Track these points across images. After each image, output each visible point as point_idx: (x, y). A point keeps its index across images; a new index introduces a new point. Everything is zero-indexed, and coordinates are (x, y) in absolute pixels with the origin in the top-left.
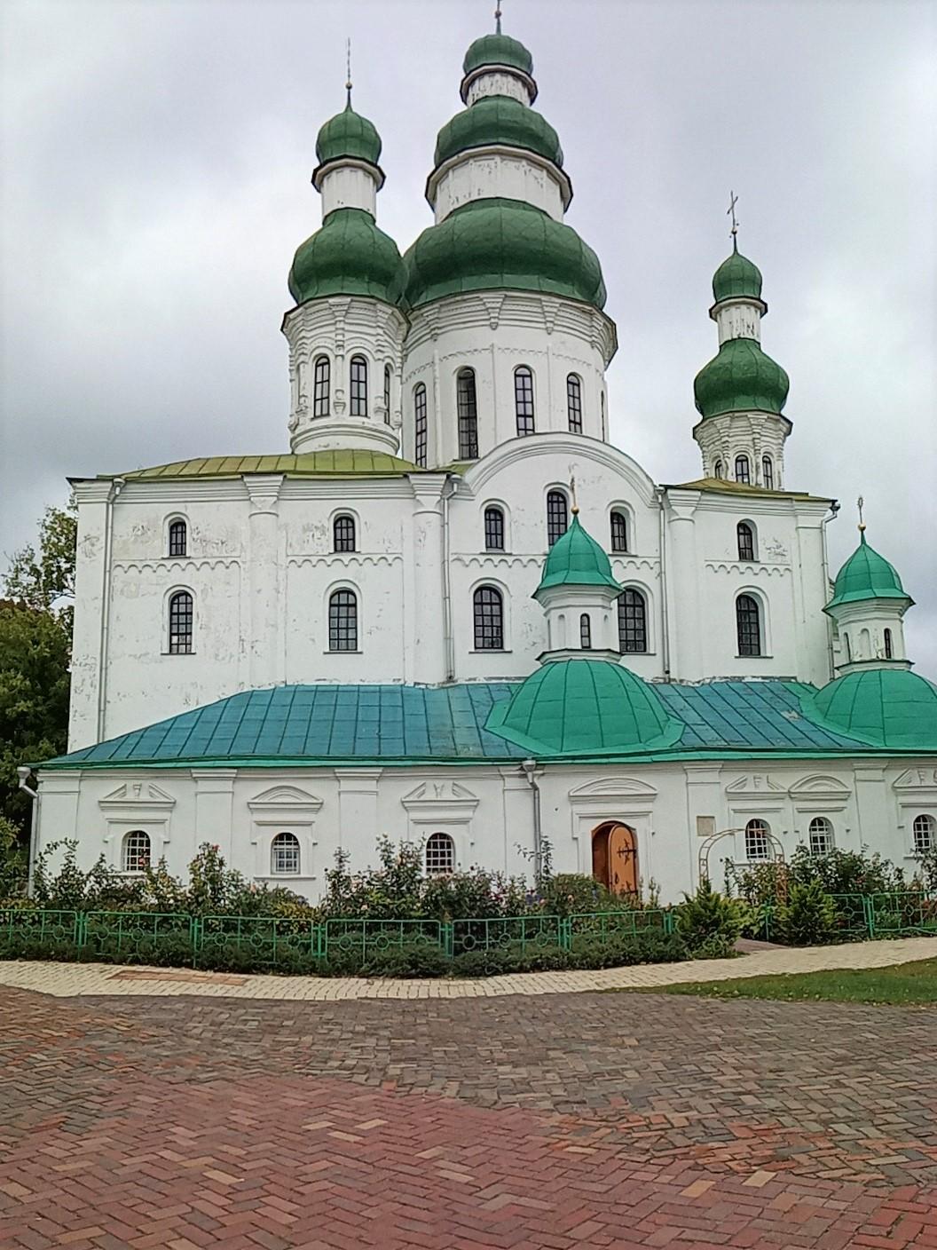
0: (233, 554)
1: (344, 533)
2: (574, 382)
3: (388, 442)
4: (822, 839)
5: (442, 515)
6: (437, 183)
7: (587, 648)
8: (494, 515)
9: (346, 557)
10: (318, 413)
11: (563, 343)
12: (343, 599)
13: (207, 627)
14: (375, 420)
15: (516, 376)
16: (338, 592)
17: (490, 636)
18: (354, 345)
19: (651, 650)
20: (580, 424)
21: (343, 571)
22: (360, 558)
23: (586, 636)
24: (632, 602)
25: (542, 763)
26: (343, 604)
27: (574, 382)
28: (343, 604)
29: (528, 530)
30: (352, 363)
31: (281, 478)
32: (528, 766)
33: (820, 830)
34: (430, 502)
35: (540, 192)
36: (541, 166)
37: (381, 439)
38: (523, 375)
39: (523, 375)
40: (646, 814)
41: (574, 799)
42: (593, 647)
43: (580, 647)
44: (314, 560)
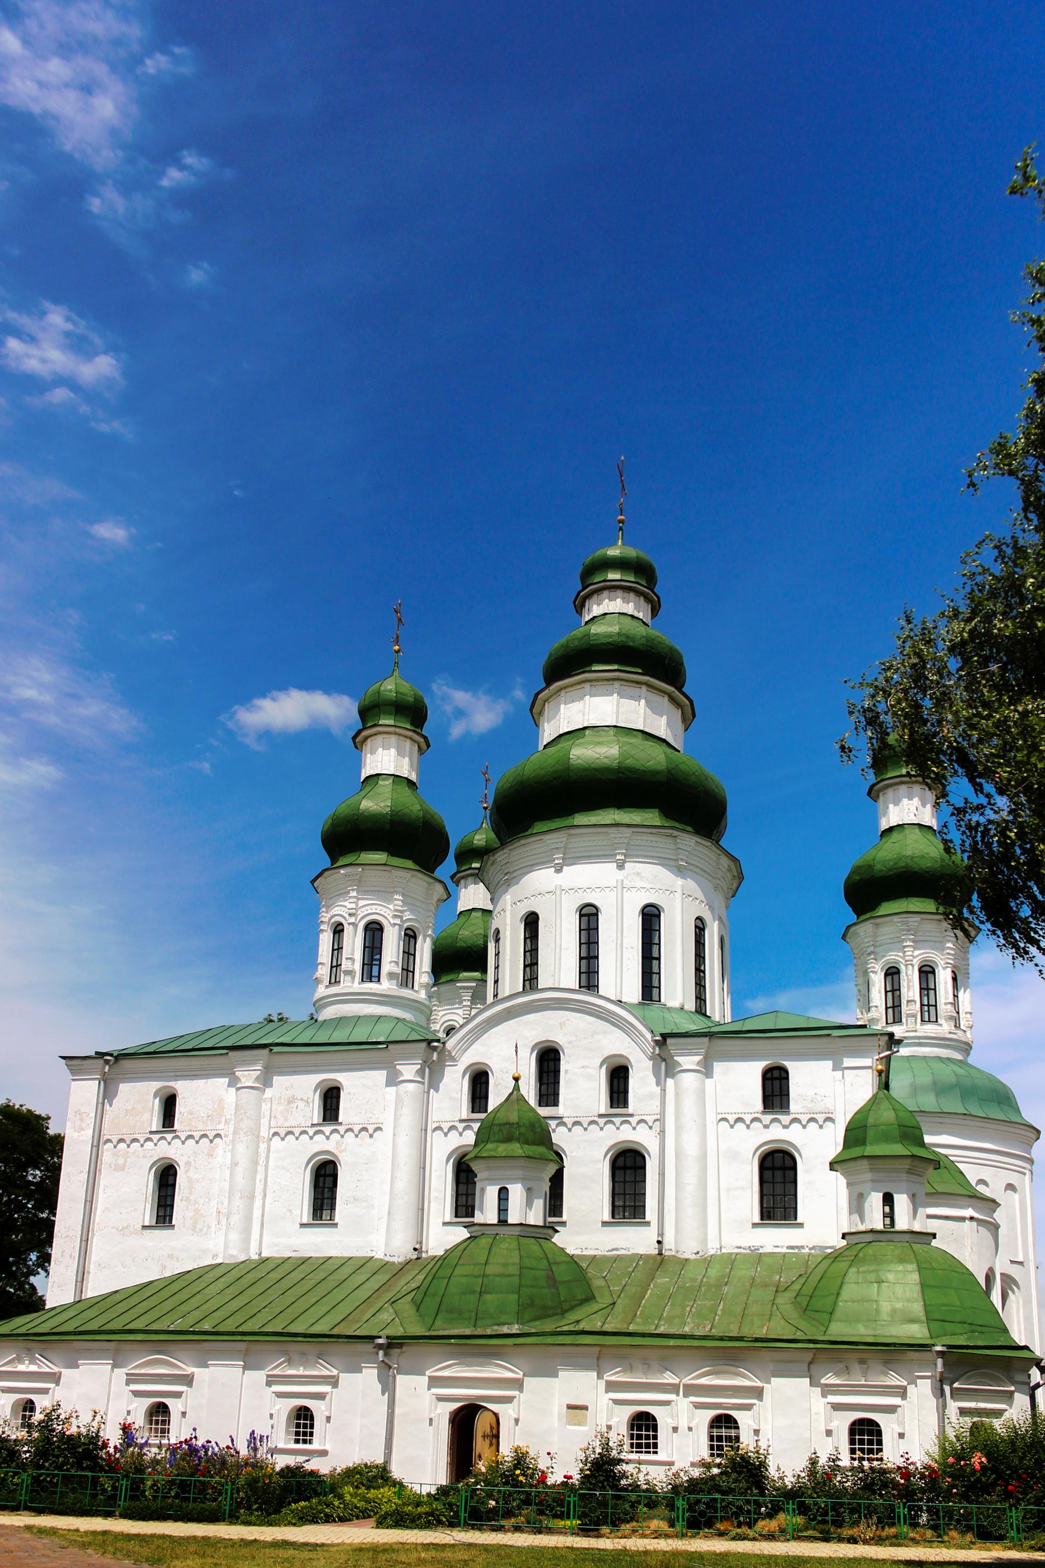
0: (218, 1127)
2: (651, 917)
4: (729, 1439)
5: (423, 1083)
7: (503, 1222)
8: (479, 1081)
10: (333, 981)
11: (638, 874)
15: (581, 916)
23: (503, 1210)
25: (394, 1344)
26: (325, 1177)
27: (651, 917)
28: (325, 1177)
32: (392, 1350)
33: (726, 1427)
34: (408, 1070)
40: (509, 1400)
41: (434, 1382)
42: (510, 1221)
43: (495, 1221)
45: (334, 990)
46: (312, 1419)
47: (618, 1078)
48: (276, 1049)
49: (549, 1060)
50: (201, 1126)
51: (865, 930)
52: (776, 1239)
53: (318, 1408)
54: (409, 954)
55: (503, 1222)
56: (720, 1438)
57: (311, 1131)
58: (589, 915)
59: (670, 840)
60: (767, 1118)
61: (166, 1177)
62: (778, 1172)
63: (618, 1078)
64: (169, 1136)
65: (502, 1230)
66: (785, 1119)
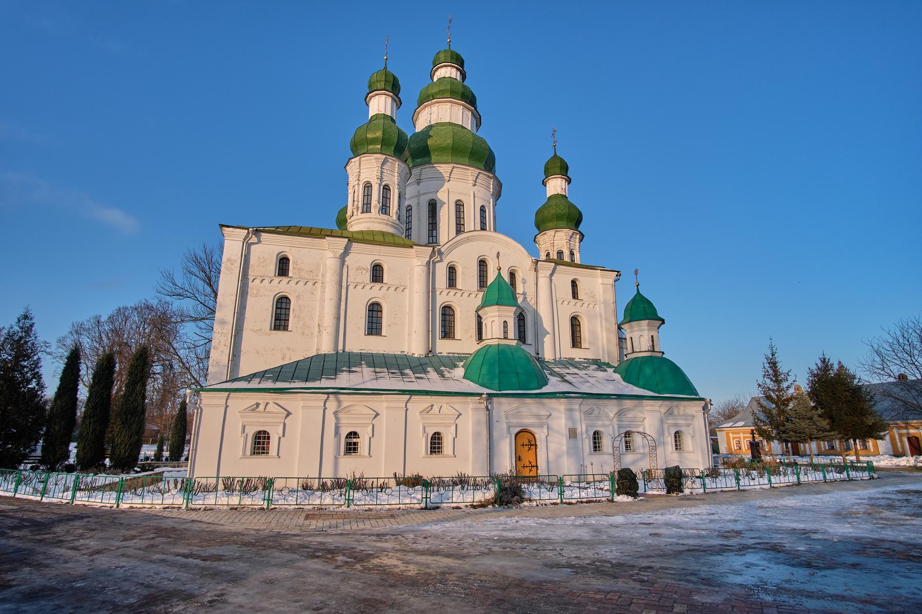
1: (377, 274)
8: (452, 270)
9: (378, 285)
16: (373, 304)
21: (375, 293)
23: (506, 332)
26: (374, 310)
27: (483, 210)
28: (374, 310)
29: (468, 278)
38: (459, 205)
39: (459, 205)
45: (365, 215)
50: (307, 277)
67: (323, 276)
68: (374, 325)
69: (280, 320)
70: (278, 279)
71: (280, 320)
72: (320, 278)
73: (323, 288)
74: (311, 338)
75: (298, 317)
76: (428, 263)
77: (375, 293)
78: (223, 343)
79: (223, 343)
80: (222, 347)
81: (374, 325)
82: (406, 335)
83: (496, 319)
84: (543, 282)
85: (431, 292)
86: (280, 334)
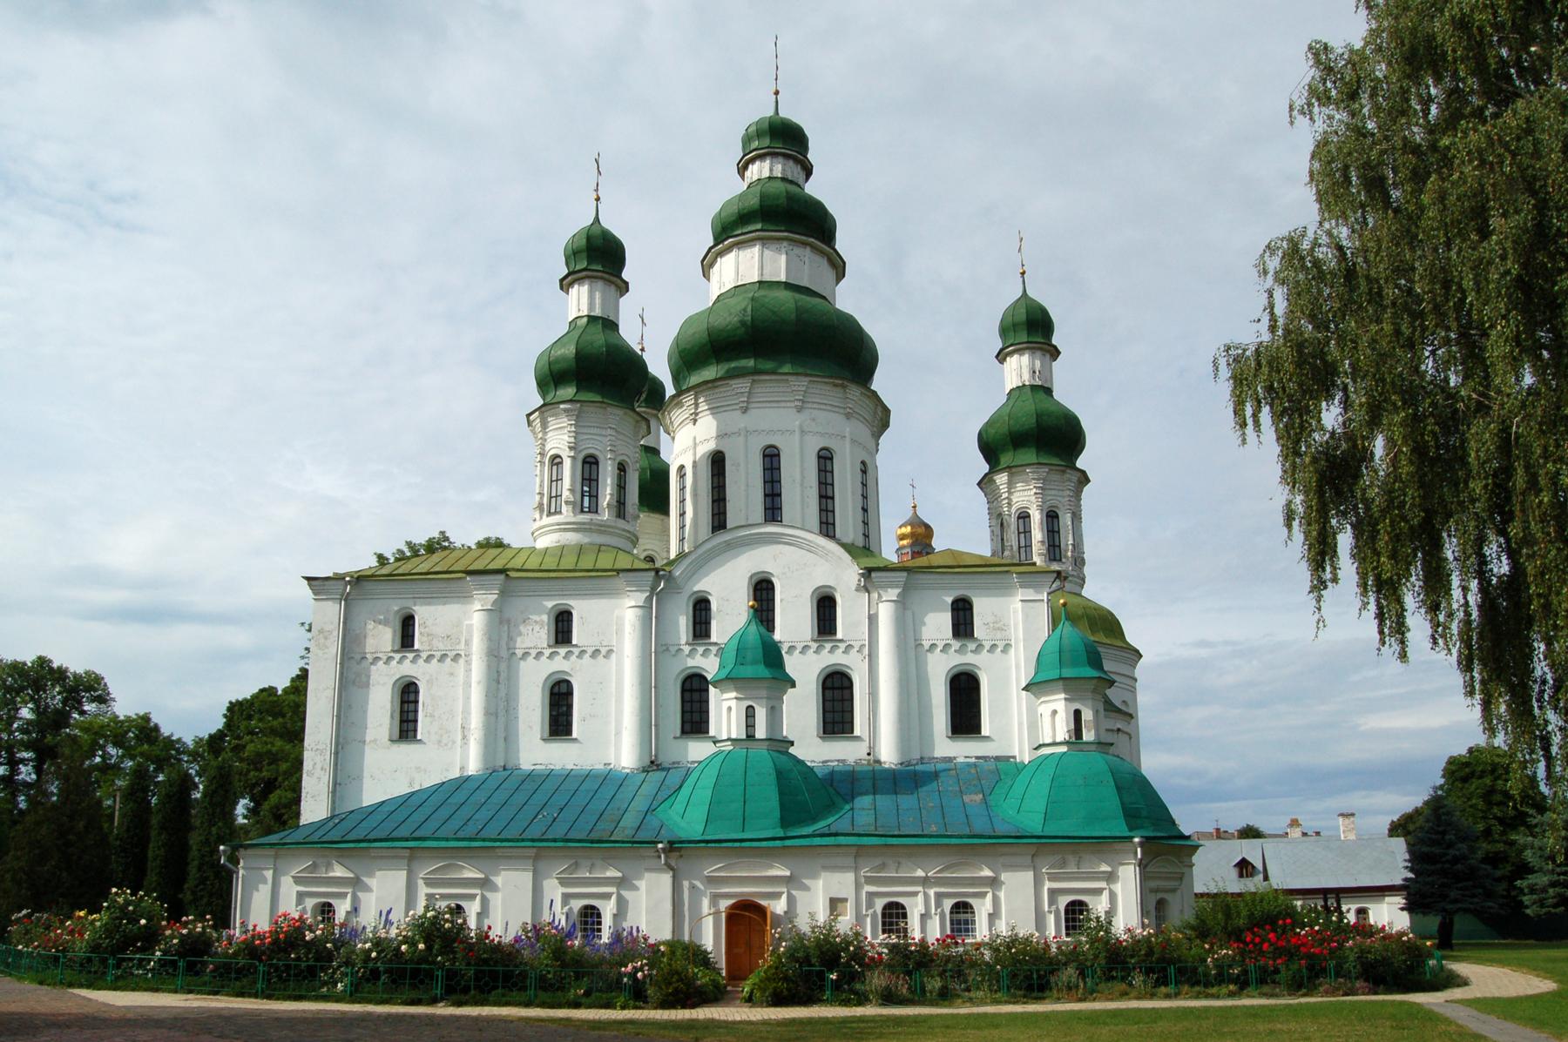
2: (825, 459)
3: (620, 536)
4: (966, 922)
6: (711, 265)
7: (750, 736)
9: (563, 651)
12: (564, 689)
13: (432, 716)
14: (605, 515)
16: (559, 683)
17: (695, 721)
18: (590, 448)
19: (857, 732)
20: (833, 498)
21: (560, 663)
22: (576, 651)
24: (836, 688)
27: (825, 459)
30: (584, 462)
31: (502, 577)
35: (811, 271)
36: (805, 244)
37: (611, 534)
38: (771, 458)
39: (771, 458)
44: (534, 652)
46: (599, 916)
47: (825, 607)
48: (512, 574)
49: (763, 590)
50: (441, 646)
51: (1001, 479)
52: (965, 750)
53: (608, 910)
54: (621, 487)
55: (750, 736)
56: (959, 922)
57: (547, 652)
58: (772, 456)
59: (839, 390)
60: (956, 644)
61: (408, 694)
62: (964, 690)
63: (825, 607)
64: (411, 656)
65: (750, 744)
66: (972, 646)
67: (468, 643)
68: (559, 722)
69: (406, 728)
70: (397, 656)
71: (406, 728)
72: (462, 646)
73: (468, 663)
74: (452, 749)
75: (432, 716)
76: (649, 599)
77: (560, 663)
78: (319, 766)
79: (319, 766)
80: (318, 772)
81: (559, 722)
82: (612, 735)
83: (733, 703)
84: (885, 612)
85: (656, 649)
86: (406, 748)
